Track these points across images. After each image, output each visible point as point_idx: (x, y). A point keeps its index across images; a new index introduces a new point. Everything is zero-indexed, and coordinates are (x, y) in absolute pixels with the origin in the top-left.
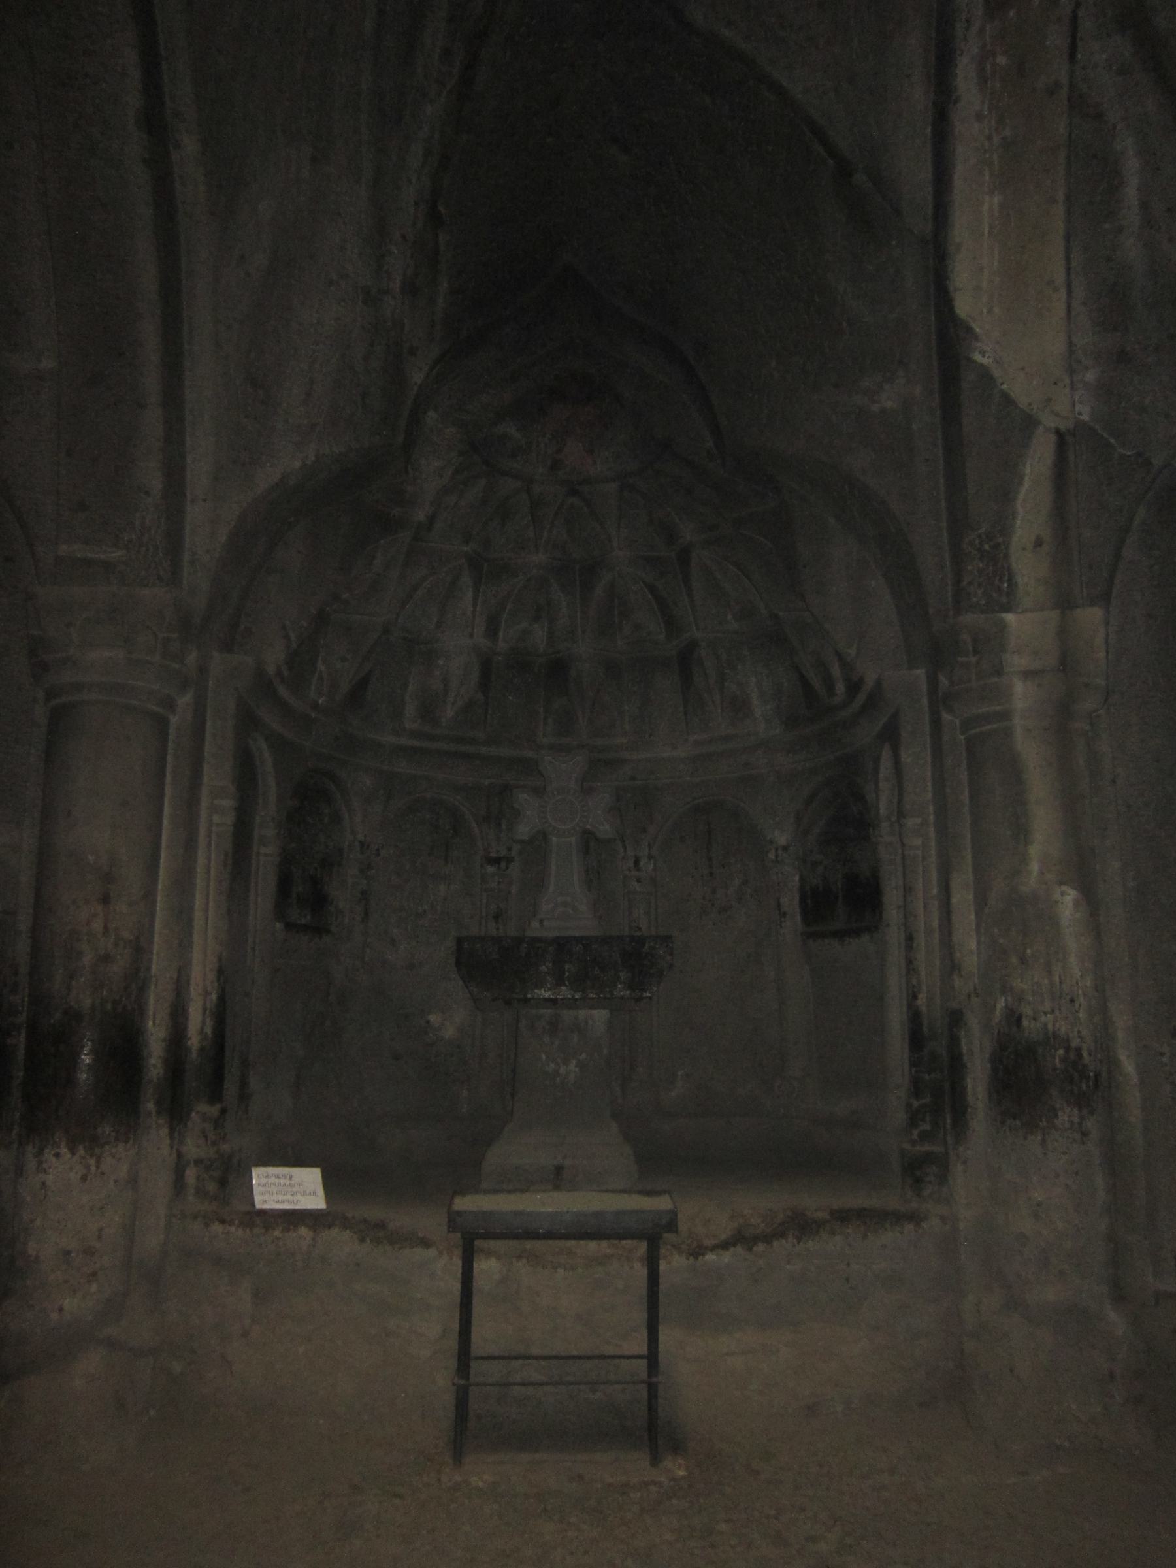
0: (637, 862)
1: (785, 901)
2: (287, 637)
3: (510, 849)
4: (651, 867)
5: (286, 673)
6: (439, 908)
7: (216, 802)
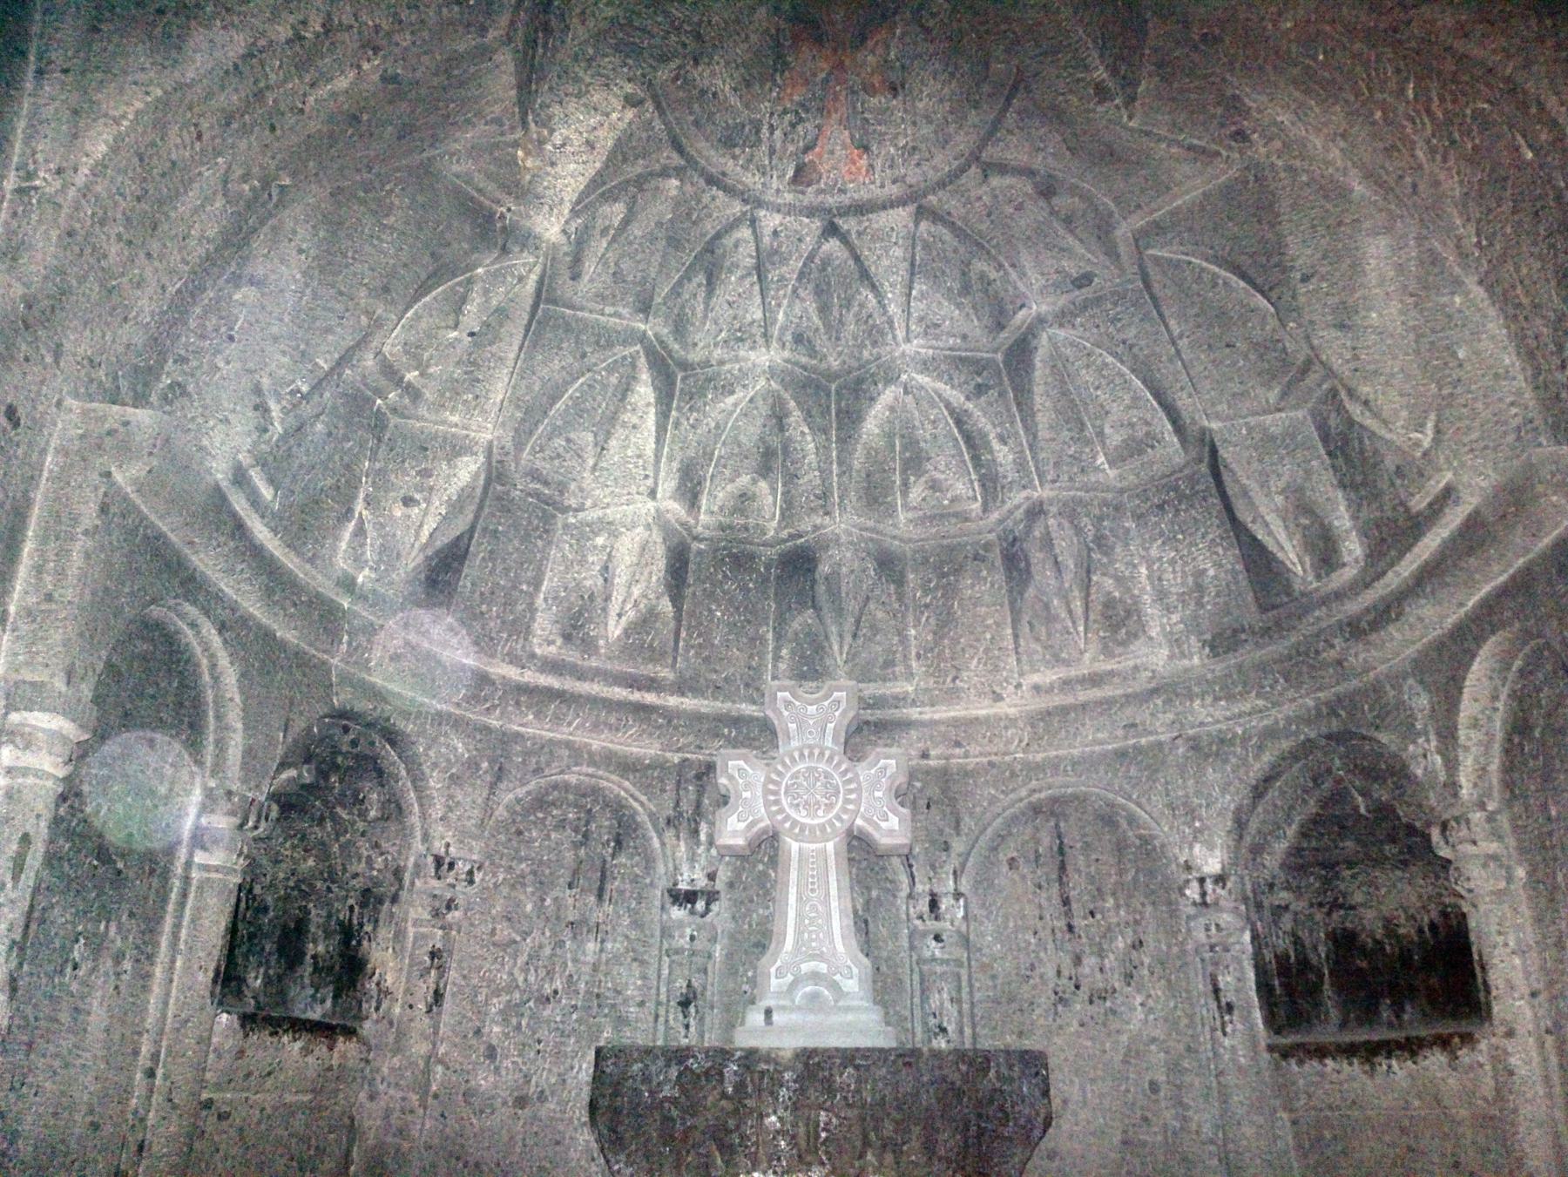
0: (934, 904)
1: (1226, 980)
2: (262, 408)
3: (712, 877)
4: (961, 914)
5: (267, 493)
7: (15, 717)
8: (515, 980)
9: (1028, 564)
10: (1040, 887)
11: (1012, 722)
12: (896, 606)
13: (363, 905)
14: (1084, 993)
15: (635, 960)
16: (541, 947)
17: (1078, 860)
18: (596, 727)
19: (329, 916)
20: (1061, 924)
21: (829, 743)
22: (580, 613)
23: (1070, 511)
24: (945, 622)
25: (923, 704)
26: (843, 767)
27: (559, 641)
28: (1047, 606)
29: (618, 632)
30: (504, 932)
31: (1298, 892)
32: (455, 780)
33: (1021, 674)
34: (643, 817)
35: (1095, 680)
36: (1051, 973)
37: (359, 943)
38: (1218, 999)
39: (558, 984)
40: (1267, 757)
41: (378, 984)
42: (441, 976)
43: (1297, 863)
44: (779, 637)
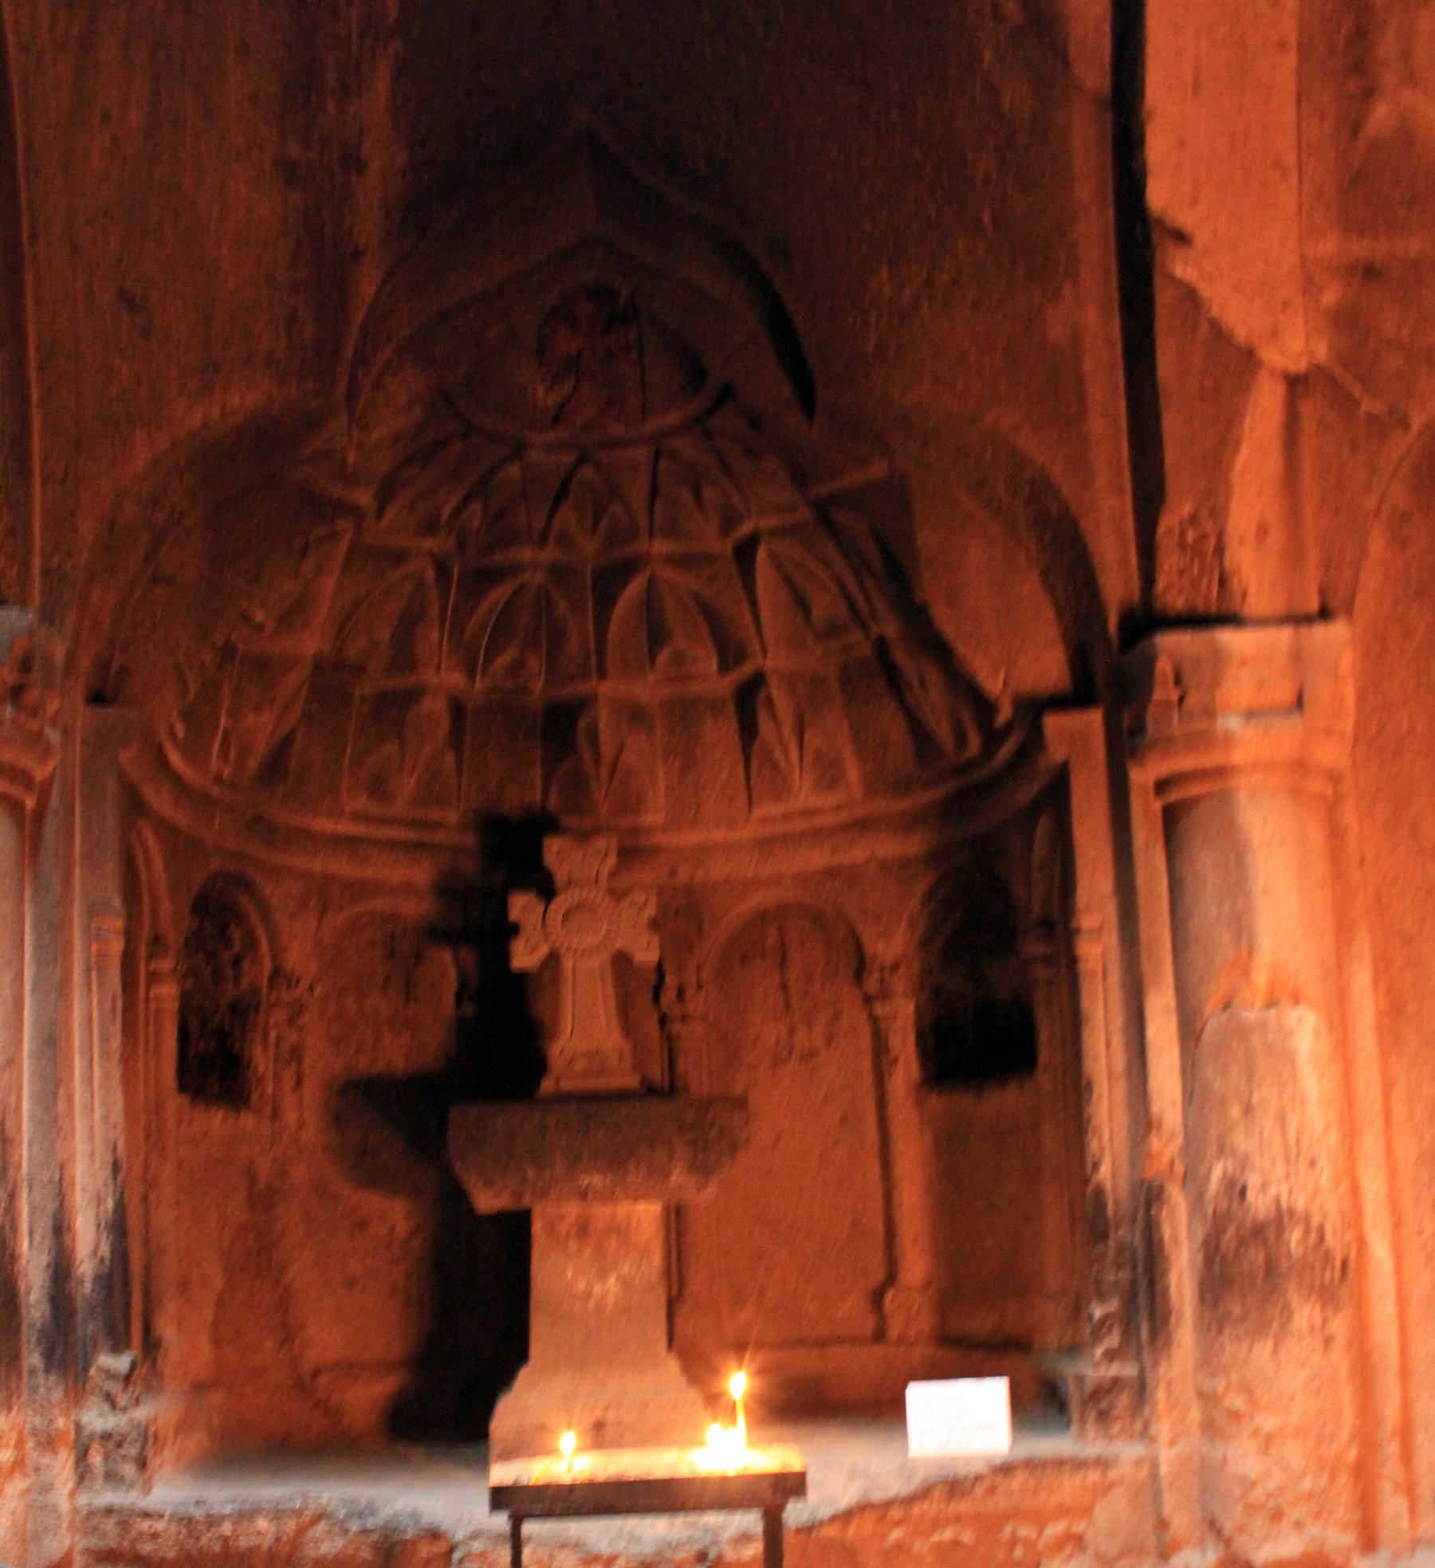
35: (809, 813)
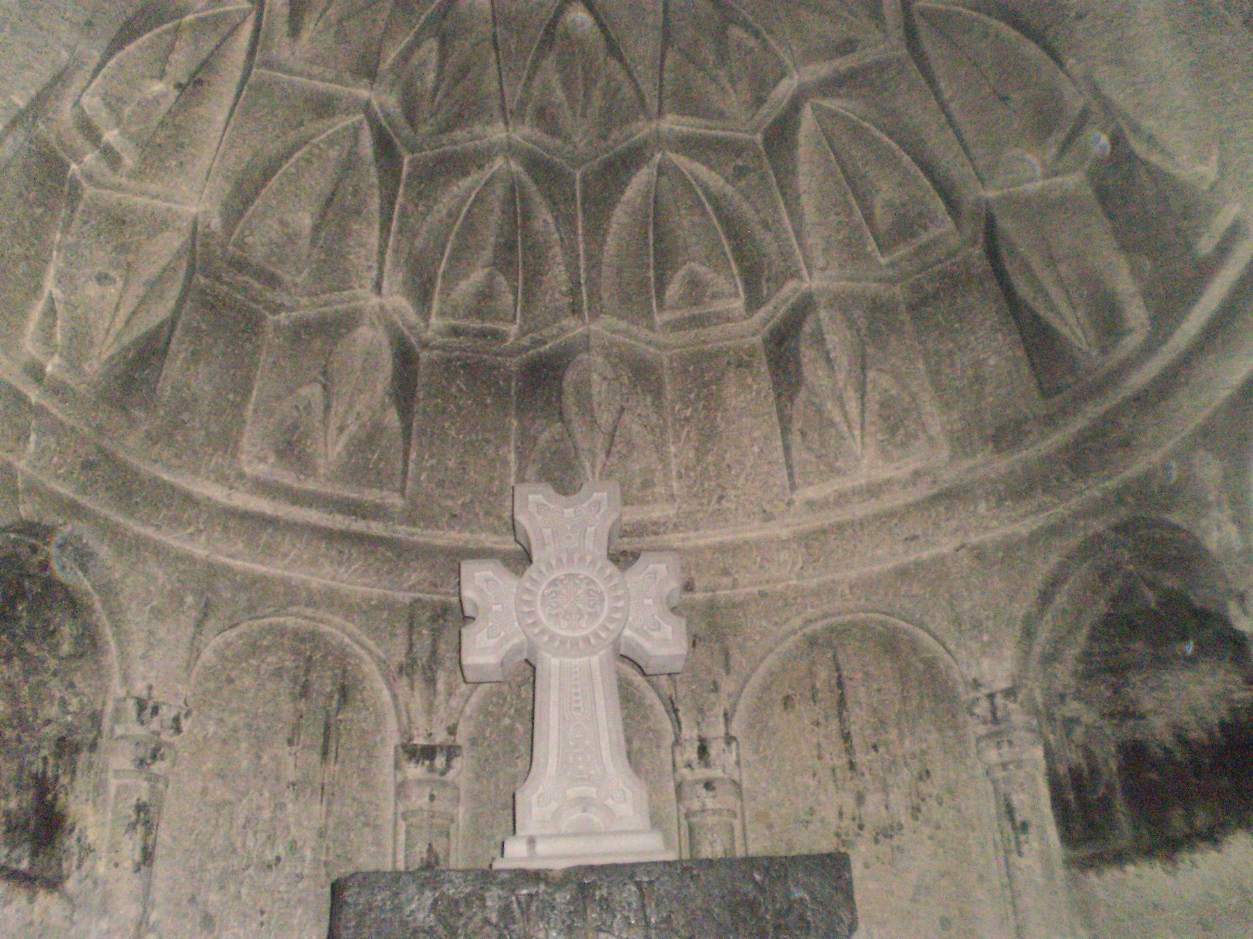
0: (703, 750)
1: (1017, 799)
3: (452, 731)
6: (308, 853)
8: (232, 844)
9: (798, 364)
10: (818, 724)
11: (784, 544)
12: (654, 419)
13: (59, 756)
14: (867, 834)
15: (366, 824)
16: (259, 808)
17: (858, 693)
18: (314, 562)
19: (21, 769)
20: (842, 762)
21: (589, 544)
22: (295, 427)
23: (842, 303)
24: (708, 436)
25: (687, 529)
26: (608, 572)
27: (272, 460)
28: (820, 411)
29: (338, 449)
30: (219, 791)
31: (1089, 703)
32: (157, 613)
33: (793, 487)
34: (370, 668)
35: (873, 490)
36: (832, 816)
37: (55, 798)
38: (1012, 819)
39: (281, 850)
40: (1054, 559)
41: (79, 840)
42: (148, 833)
43: (1090, 670)
44: (521, 456)
